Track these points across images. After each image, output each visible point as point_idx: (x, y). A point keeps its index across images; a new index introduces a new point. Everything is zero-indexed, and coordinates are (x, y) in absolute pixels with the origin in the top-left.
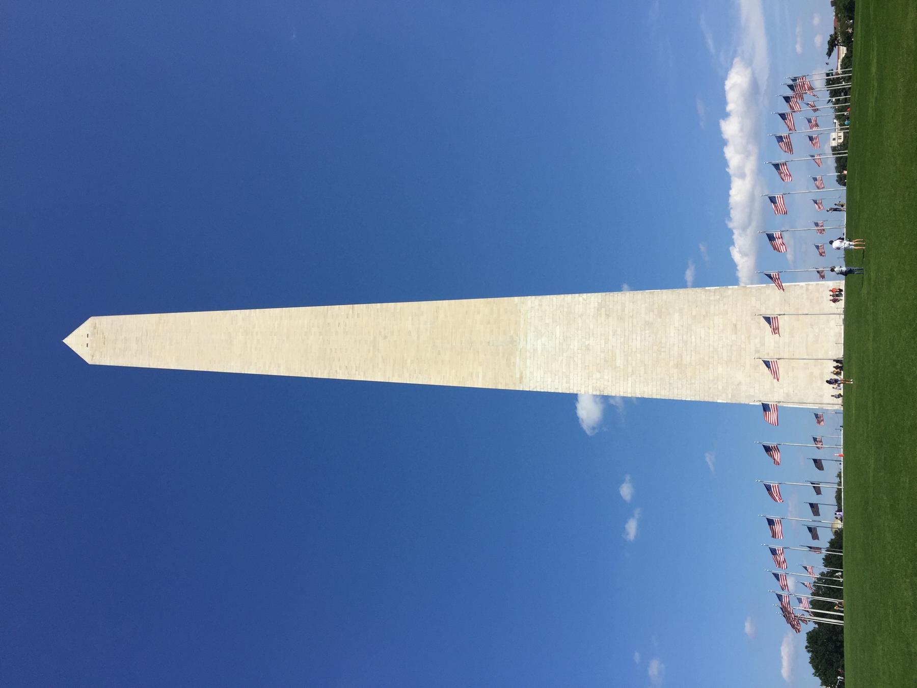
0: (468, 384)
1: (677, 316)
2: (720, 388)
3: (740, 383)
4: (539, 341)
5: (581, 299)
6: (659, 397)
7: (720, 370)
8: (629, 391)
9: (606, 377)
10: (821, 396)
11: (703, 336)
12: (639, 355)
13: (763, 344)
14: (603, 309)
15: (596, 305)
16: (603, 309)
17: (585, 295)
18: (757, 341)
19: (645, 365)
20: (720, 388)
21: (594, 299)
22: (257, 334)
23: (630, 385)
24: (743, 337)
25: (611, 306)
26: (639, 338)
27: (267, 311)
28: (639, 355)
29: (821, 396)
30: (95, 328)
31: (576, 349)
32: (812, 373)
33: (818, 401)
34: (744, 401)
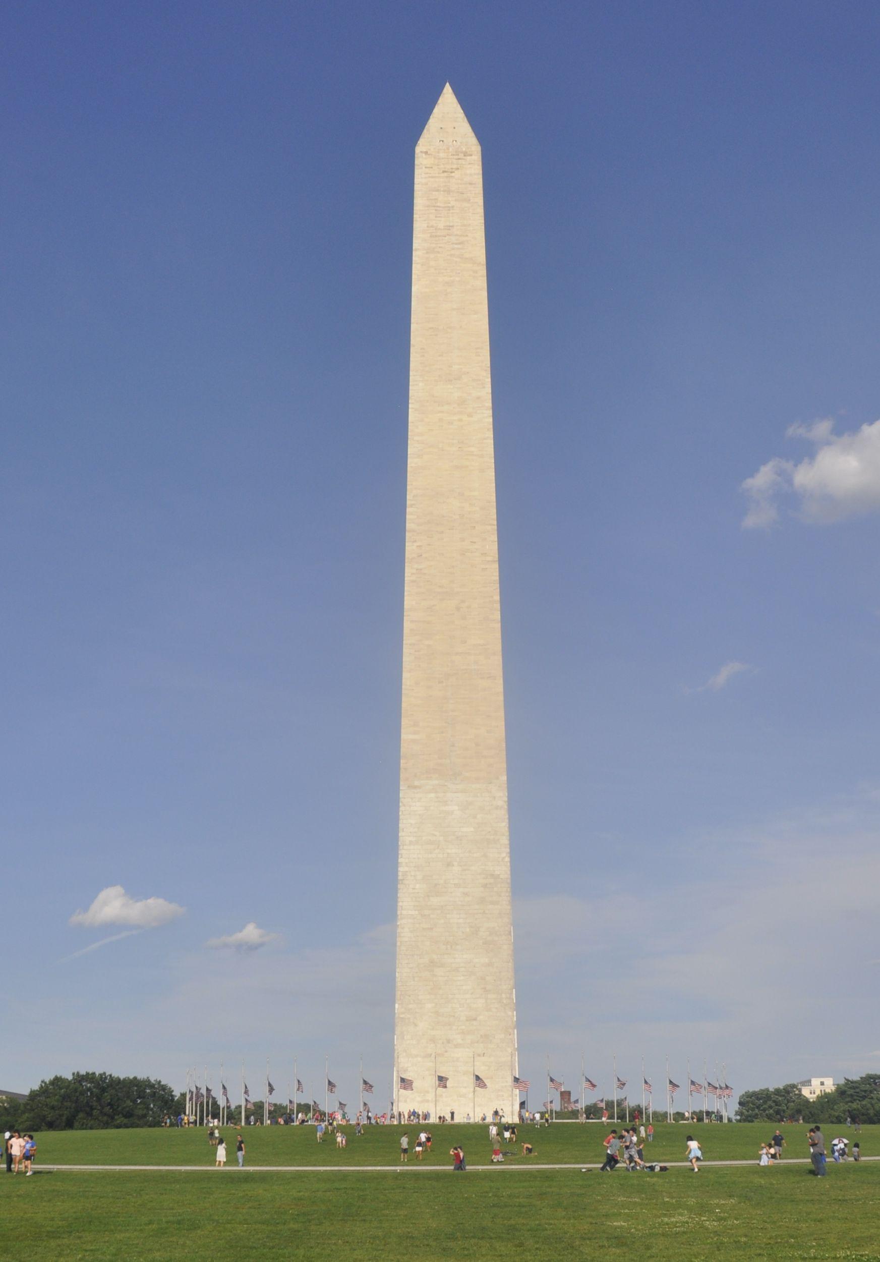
0: (405, 722)
1: (487, 960)
2: (411, 1006)
3: (416, 1025)
4: (456, 808)
5: (504, 855)
6: (398, 944)
7: (429, 1006)
8: (404, 912)
9: (418, 886)
10: (406, 1101)
11: (464, 987)
12: (442, 921)
13: (456, 1046)
14: (492, 881)
15: (497, 873)
16: (492, 881)
17: (507, 859)
18: (460, 1041)
19: (432, 929)
20: (411, 1006)
21: (503, 870)
22: (460, 420)
23: (410, 912)
24: (463, 1027)
25: (495, 889)
26: (461, 921)
27: (490, 434)
28: (442, 921)
29: (406, 1101)
30: (465, 154)
31: (449, 851)
32: (428, 1092)
33: (401, 1099)
34: (398, 1030)
